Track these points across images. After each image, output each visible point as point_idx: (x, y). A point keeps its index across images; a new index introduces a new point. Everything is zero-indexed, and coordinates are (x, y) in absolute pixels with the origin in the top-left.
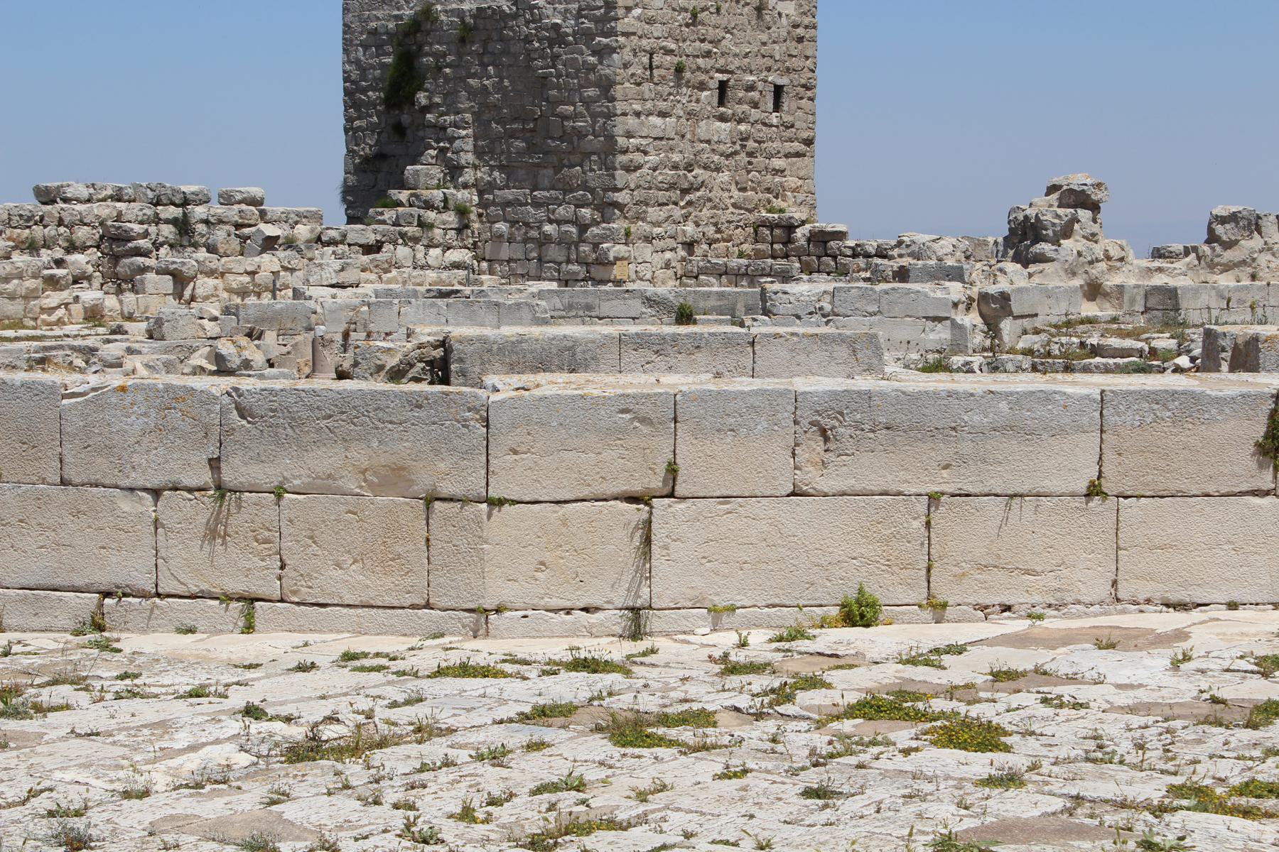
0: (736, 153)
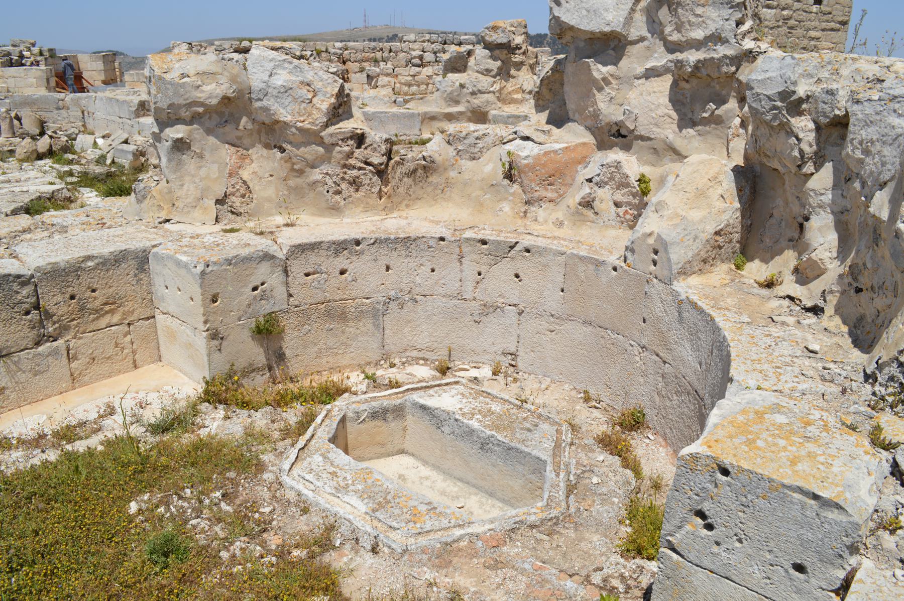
0: (778, 27)
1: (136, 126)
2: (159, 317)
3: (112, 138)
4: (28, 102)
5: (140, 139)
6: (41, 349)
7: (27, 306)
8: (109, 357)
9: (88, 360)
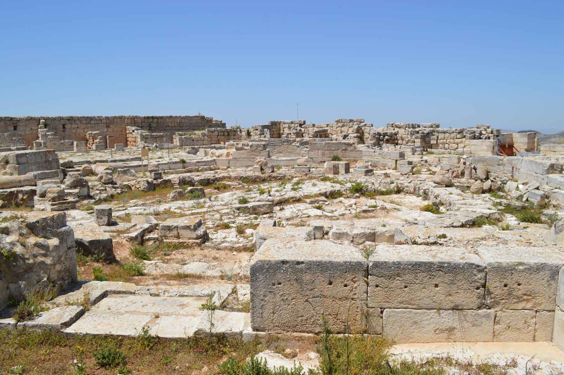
1: (546, 179)
2: (558, 312)
3: (529, 185)
4: (482, 160)
5: (547, 188)
6: (480, 311)
7: (479, 284)
8: (519, 329)
9: (505, 326)
